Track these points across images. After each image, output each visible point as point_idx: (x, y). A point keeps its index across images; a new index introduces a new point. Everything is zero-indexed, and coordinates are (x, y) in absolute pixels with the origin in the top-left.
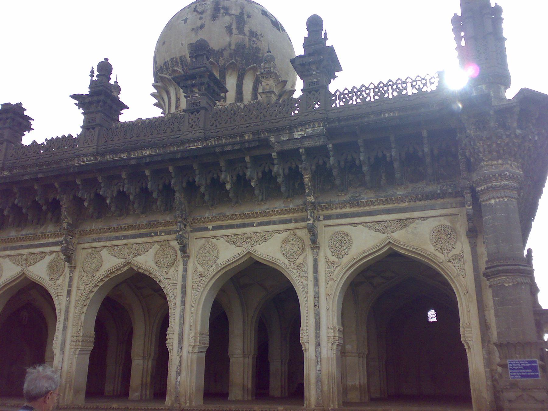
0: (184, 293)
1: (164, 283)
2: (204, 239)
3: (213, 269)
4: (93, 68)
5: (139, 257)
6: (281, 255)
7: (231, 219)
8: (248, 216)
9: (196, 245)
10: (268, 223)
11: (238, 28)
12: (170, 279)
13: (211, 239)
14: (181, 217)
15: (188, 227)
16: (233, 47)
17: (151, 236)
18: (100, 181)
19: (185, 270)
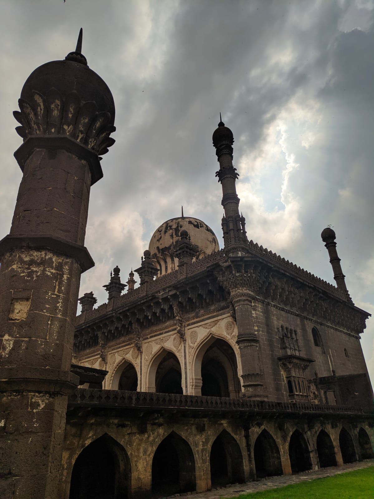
0: (141, 369)
1: (135, 365)
2: (147, 343)
3: (151, 356)
4: (111, 272)
5: (127, 355)
6: (173, 346)
7: (156, 332)
8: (161, 330)
9: (144, 347)
10: (168, 332)
11: (176, 234)
12: (136, 363)
13: (150, 343)
14: (136, 335)
15: (141, 339)
16: (174, 244)
17: (130, 345)
18: (122, 318)
19: (141, 359)
